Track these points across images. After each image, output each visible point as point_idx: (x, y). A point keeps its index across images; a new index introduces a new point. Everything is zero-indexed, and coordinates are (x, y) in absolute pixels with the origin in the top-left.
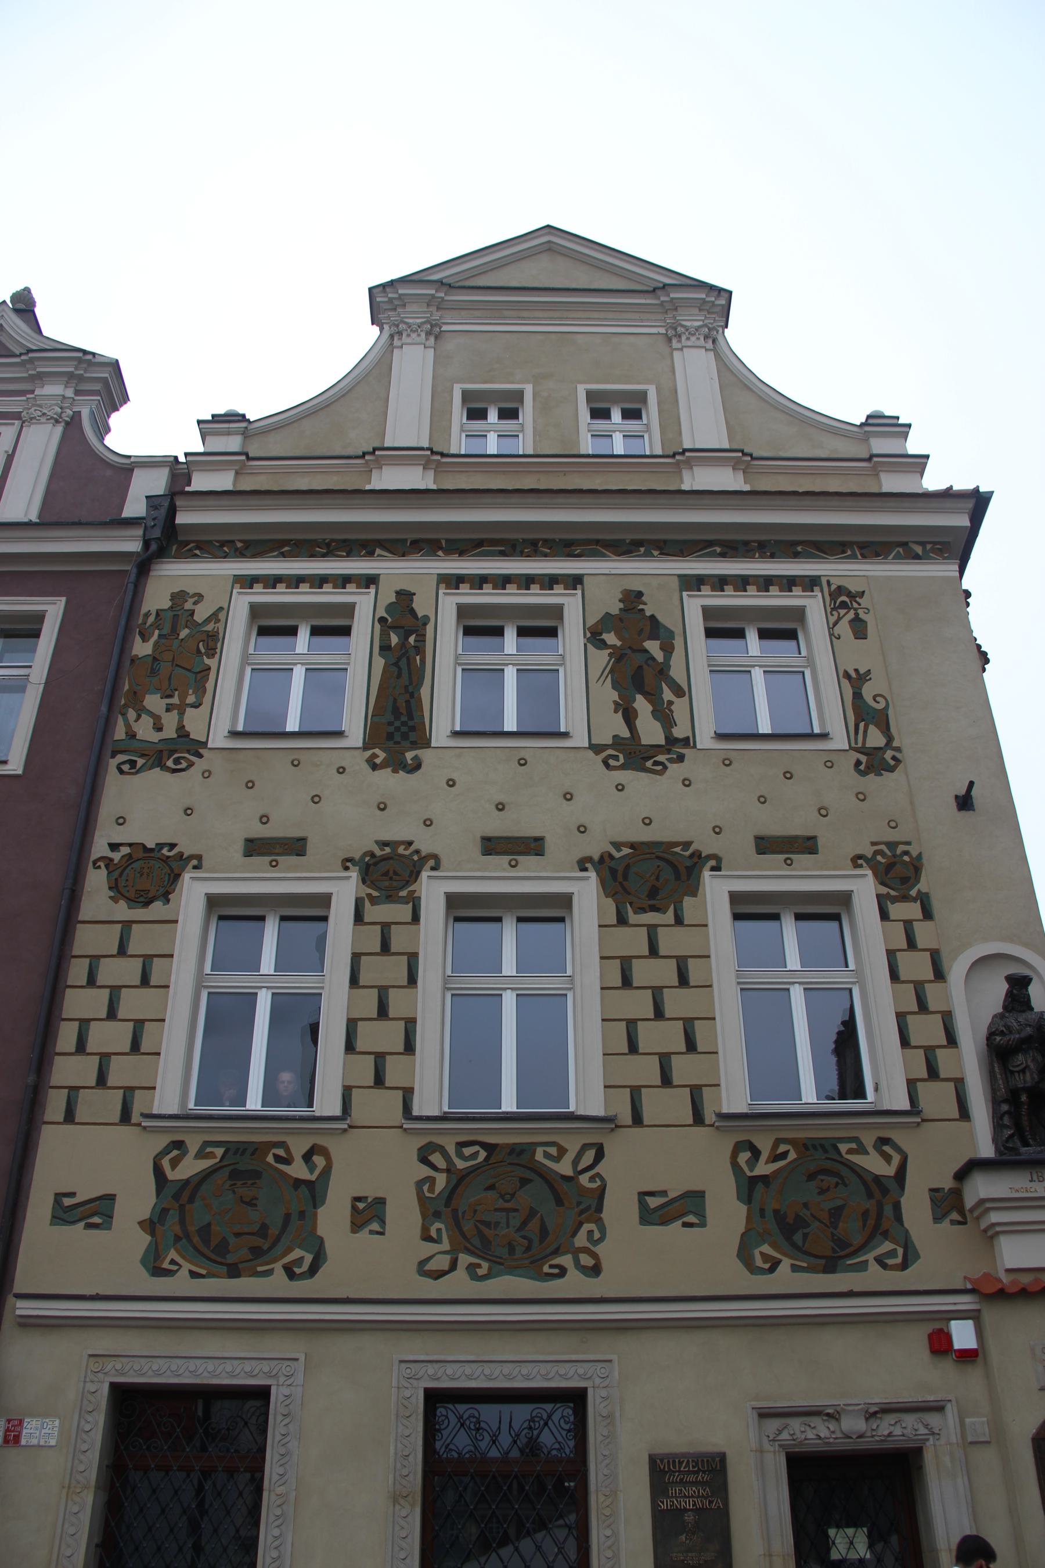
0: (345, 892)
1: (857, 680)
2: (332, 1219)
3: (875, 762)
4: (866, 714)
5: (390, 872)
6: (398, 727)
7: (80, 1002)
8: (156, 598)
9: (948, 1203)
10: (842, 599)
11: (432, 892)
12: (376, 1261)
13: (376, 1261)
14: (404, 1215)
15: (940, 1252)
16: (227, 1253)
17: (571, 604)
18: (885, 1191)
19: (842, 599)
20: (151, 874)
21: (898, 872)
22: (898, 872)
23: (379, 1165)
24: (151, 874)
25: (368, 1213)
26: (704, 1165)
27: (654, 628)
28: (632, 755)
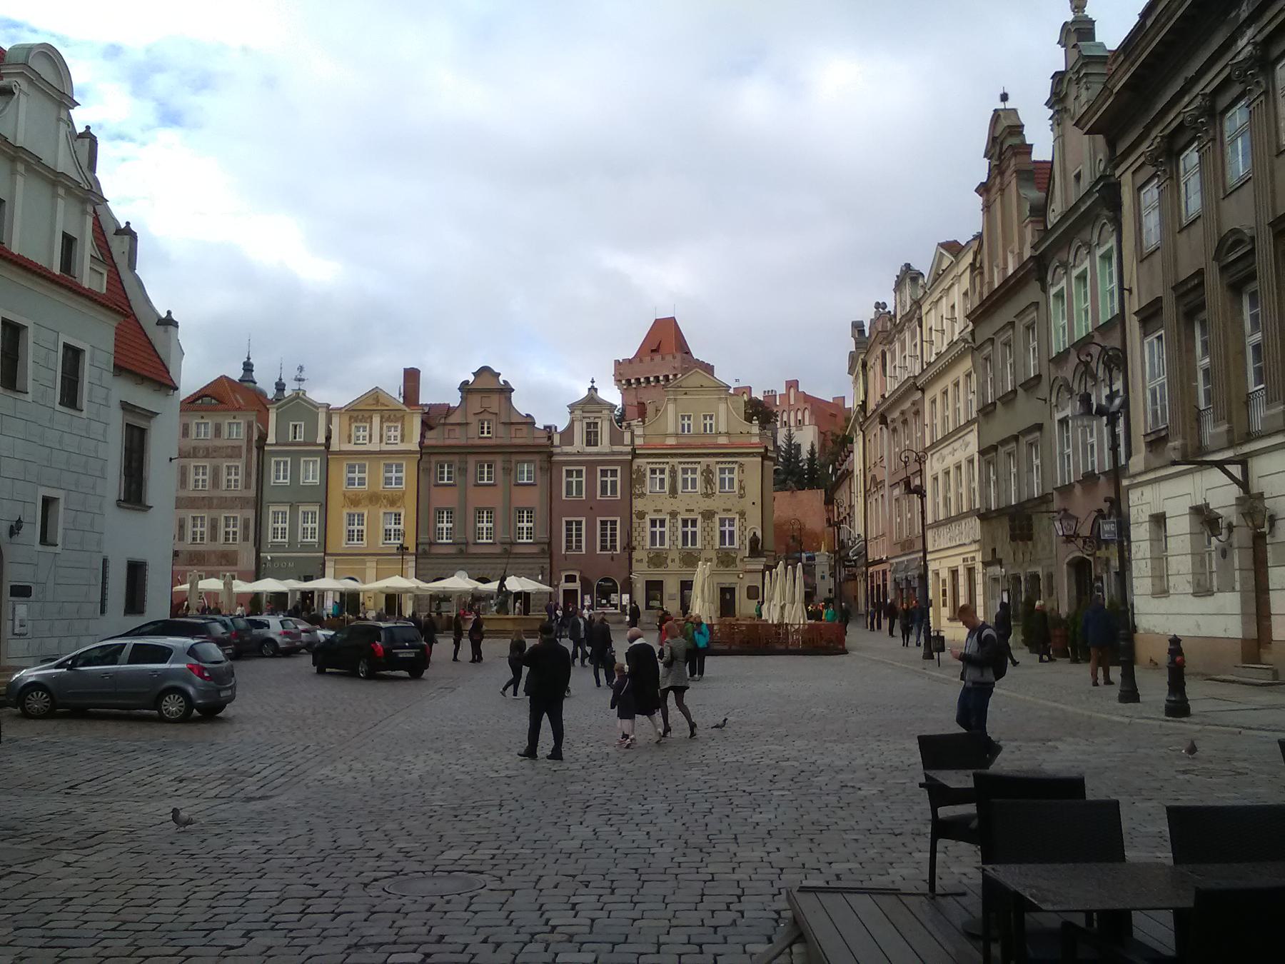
0: (668, 518)
1: (741, 482)
2: (669, 561)
3: (741, 496)
4: (742, 488)
5: (673, 515)
6: (673, 491)
7: (635, 534)
8: (635, 467)
9: (742, 560)
10: (741, 465)
11: (679, 518)
12: (674, 566)
13: (674, 566)
14: (677, 560)
15: (740, 566)
16: (656, 566)
17: (698, 466)
18: (734, 559)
19: (741, 465)
20: (641, 515)
21: (742, 514)
22: (742, 514)
23: (674, 555)
24: (641, 515)
25: (673, 561)
26: (713, 555)
27: (711, 472)
28: (707, 495)
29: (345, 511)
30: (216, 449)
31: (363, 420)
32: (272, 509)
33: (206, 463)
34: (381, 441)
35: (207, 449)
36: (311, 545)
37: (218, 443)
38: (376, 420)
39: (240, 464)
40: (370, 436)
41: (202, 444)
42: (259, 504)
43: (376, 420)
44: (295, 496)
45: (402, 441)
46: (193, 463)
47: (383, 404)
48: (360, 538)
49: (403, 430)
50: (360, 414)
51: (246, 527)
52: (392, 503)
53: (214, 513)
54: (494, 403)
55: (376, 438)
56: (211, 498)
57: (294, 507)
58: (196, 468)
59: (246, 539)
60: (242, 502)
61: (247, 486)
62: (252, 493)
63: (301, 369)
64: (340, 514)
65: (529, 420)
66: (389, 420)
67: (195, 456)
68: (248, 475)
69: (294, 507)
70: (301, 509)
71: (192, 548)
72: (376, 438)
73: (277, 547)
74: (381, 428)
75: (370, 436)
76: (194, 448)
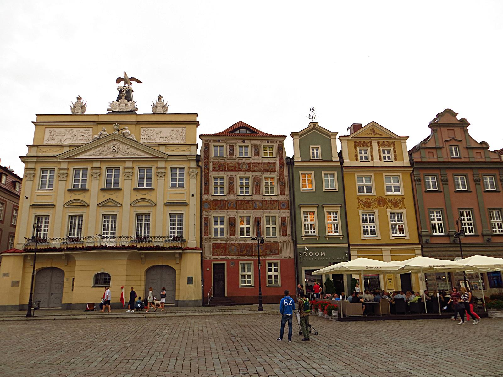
29: (360, 212)
30: (256, 165)
31: (365, 144)
32: (303, 210)
33: (249, 175)
34: (380, 160)
35: (249, 164)
36: (337, 238)
37: (257, 160)
38: (375, 145)
39: (276, 175)
40: (372, 156)
41: (244, 160)
42: (292, 206)
43: (375, 145)
44: (321, 201)
45: (396, 160)
46: (239, 175)
47: (378, 134)
48: (373, 231)
49: (395, 151)
50: (362, 140)
51: (284, 224)
52: (396, 205)
53: (258, 213)
54: (458, 134)
55: (376, 157)
56: (255, 201)
57: (320, 208)
58: (241, 178)
59: (284, 233)
60: (280, 205)
61: (282, 192)
62: (286, 198)
63: (313, 110)
64: (356, 213)
65: (484, 146)
66: (383, 144)
67: (240, 170)
68: (282, 184)
69: (320, 208)
70: (326, 210)
71: (242, 241)
72: (376, 157)
73: (310, 239)
74: (379, 150)
75: (372, 156)
76: (239, 164)
